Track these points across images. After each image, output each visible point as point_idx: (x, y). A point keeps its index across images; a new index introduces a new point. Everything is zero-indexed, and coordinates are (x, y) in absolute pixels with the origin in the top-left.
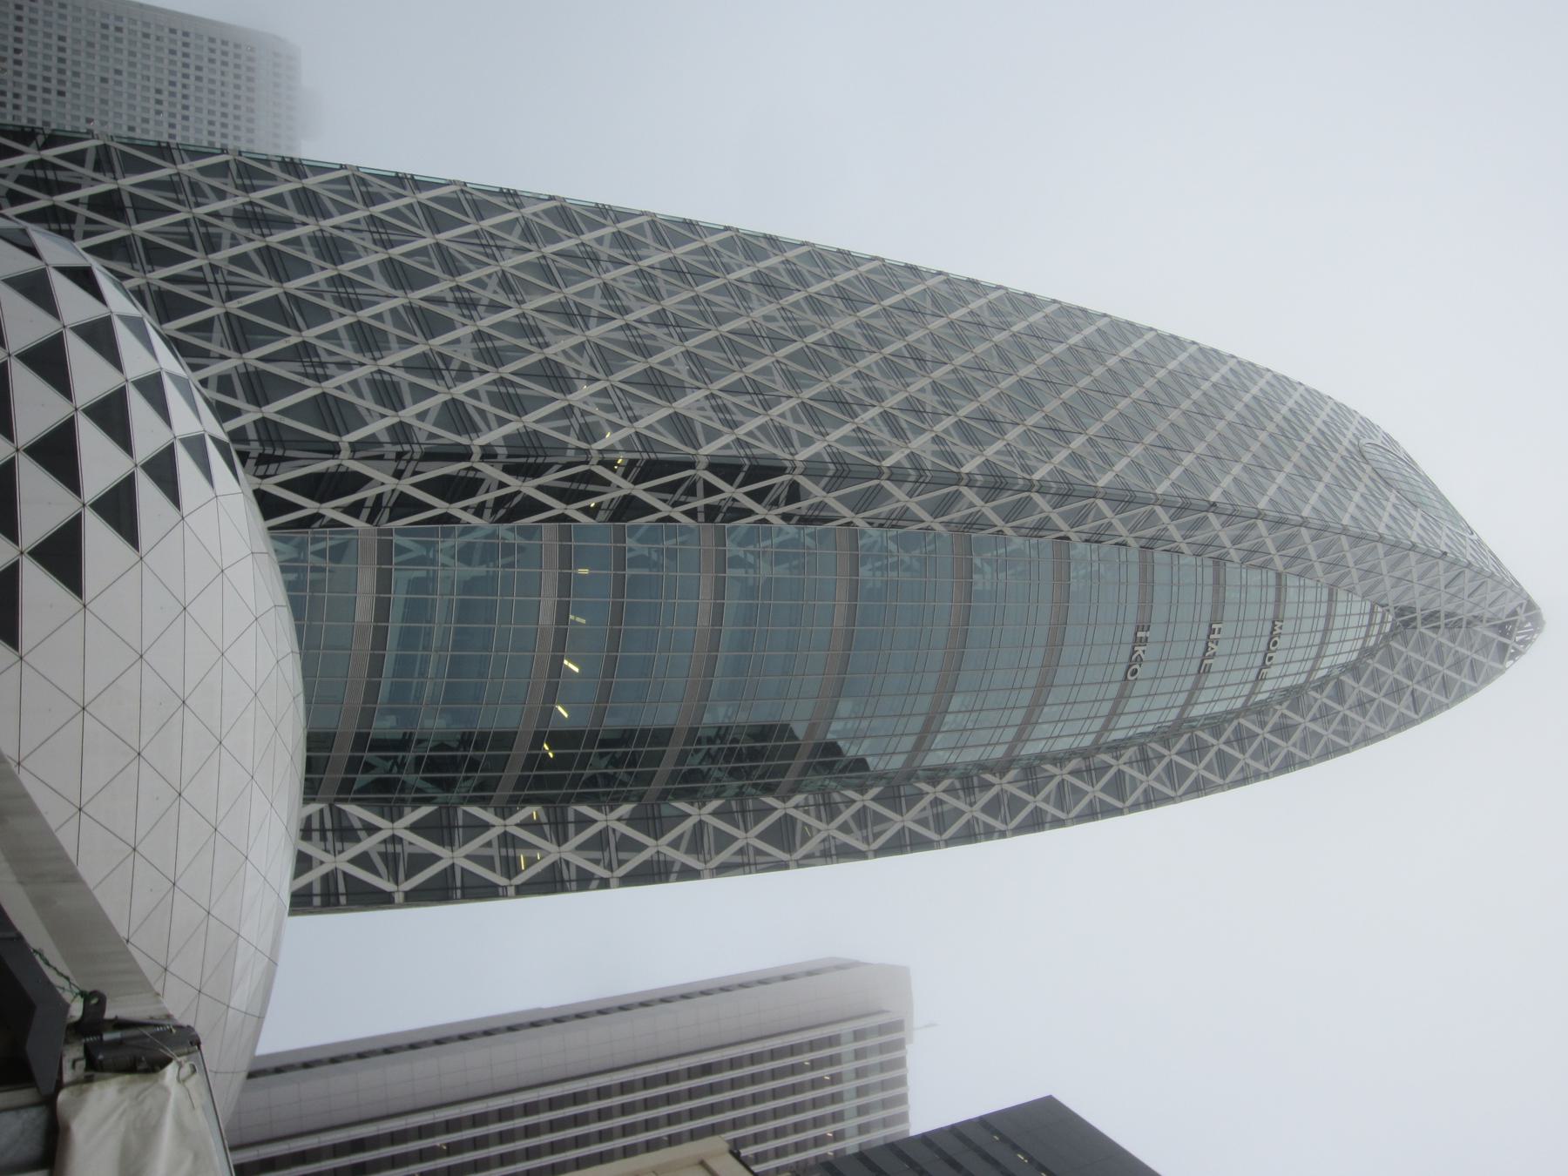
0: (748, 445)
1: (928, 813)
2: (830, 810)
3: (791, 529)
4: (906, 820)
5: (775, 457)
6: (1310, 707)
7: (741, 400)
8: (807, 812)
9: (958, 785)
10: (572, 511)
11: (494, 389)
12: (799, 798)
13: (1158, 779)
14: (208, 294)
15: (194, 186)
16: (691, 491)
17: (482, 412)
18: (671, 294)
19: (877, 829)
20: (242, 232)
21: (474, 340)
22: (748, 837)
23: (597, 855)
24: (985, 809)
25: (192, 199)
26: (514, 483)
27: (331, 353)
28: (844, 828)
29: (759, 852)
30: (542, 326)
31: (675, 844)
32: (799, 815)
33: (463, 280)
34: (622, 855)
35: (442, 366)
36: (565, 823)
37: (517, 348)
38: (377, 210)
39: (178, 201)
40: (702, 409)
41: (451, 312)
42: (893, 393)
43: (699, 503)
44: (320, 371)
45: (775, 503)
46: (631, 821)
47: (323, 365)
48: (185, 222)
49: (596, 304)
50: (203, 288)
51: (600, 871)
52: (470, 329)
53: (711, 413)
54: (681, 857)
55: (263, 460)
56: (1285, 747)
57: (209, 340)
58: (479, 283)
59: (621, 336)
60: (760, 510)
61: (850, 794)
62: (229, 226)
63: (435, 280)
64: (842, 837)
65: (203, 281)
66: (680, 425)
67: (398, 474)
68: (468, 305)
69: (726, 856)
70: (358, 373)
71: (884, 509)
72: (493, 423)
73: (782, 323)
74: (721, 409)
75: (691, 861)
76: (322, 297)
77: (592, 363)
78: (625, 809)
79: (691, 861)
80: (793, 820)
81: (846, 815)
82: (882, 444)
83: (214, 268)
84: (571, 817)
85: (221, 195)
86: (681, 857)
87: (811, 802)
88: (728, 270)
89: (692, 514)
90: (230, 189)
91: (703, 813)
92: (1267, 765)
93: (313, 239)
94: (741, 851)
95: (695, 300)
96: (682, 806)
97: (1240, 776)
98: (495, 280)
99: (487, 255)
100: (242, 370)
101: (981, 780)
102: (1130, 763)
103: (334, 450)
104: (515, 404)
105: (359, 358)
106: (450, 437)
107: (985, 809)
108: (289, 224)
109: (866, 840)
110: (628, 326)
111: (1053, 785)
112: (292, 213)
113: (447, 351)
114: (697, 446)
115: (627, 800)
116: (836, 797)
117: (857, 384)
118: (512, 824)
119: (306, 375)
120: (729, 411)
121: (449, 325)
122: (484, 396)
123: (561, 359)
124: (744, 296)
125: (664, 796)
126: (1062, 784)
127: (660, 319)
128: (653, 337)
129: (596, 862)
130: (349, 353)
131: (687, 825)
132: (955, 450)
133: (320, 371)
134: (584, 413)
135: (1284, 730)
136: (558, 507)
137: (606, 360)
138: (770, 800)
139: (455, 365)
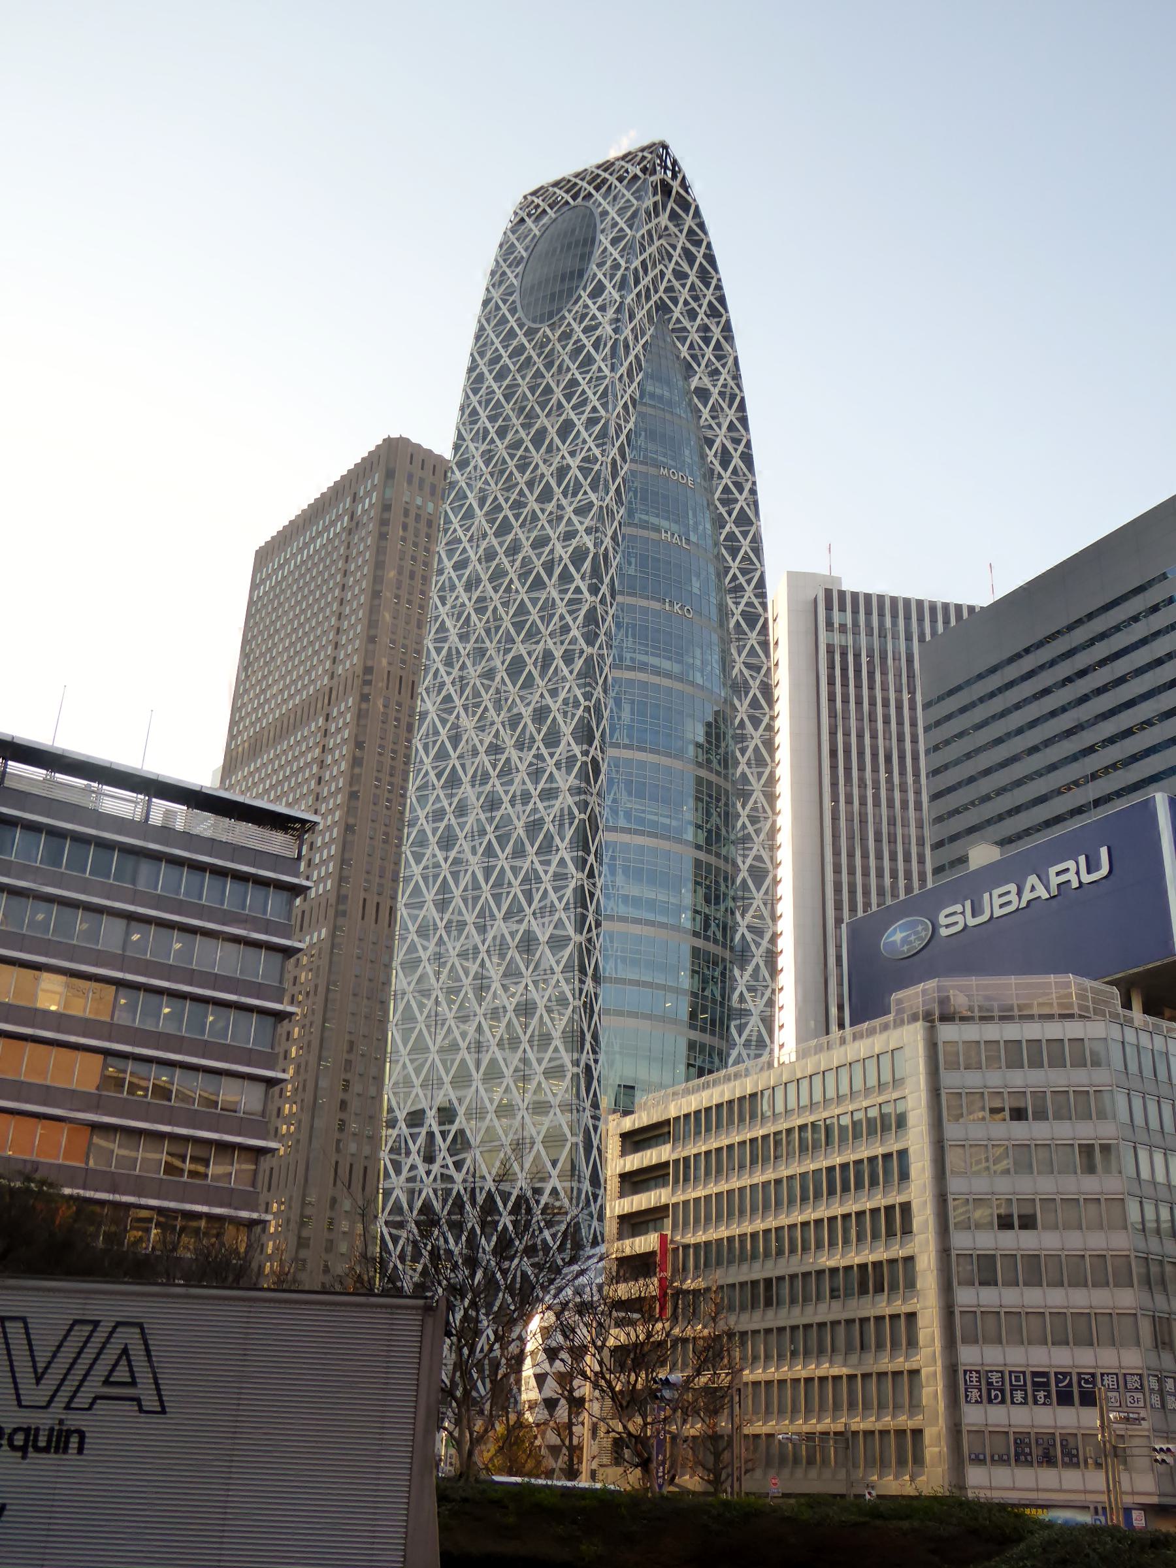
0: (567, 903)
1: (755, 770)
2: (747, 838)
3: (605, 869)
4: (757, 786)
5: (575, 890)
6: (710, 427)
7: (537, 897)
9: (740, 746)
10: (596, 1009)
11: (535, 1048)
12: (739, 860)
13: (749, 582)
14: (481, 1189)
15: (408, 1180)
16: (589, 940)
17: (551, 1060)
18: (460, 913)
19: (761, 810)
20: (439, 1162)
22: (758, 897)
23: (759, 993)
24: (756, 729)
25: (418, 1183)
26: (588, 1046)
29: (766, 893)
31: (758, 945)
32: (749, 861)
33: (463, 1045)
34: (761, 979)
36: (741, 1010)
38: (417, 1082)
39: (420, 1192)
40: (543, 924)
42: (524, 783)
45: (594, 885)
46: (742, 969)
48: (435, 1191)
49: (474, 968)
50: (478, 1190)
51: (768, 993)
52: (496, 1049)
53: (546, 920)
54: (765, 943)
55: (579, 1182)
56: (736, 461)
57: (510, 1194)
58: (464, 1035)
60: (598, 893)
61: (739, 824)
62: (436, 1168)
63: (463, 1061)
64: (762, 836)
65: (473, 1190)
66: (557, 943)
67: (584, 1109)
68: (479, 1047)
69: (766, 914)
70: (528, 1120)
72: (555, 1055)
73: (477, 843)
75: (768, 936)
77: (516, 983)
78: (737, 972)
79: (768, 936)
80: (751, 866)
81: (750, 829)
82: (562, 810)
83: (465, 1181)
84: (738, 1006)
85: (413, 1167)
86: (765, 943)
87: (741, 852)
88: (437, 865)
90: (410, 1161)
91: (743, 923)
92: (747, 480)
93: (441, 1123)
94: (765, 904)
95: (465, 900)
96: (738, 937)
97: (752, 507)
98: (462, 1026)
99: (443, 1025)
101: (738, 728)
102: (737, 604)
104: (544, 1040)
105: (519, 1117)
107: (756, 729)
108: (431, 1135)
109: (766, 818)
110: (488, 951)
111: (746, 672)
112: (423, 1131)
113: (512, 1069)
115: (731, 971)
116: (740, 835)
117: (519, 807)
118: (740, 1041)
121: (493, 1062)
122: (541, 1055)
123: (514, 1001)
124: (456, 862)
125: (732, 949)
126: (748, 666)
127: (482, 929)
128: (494, 938)
129: (763, 994)
131: (749, 936)
132: (564, 755)
134: (549, 1000)
135: (725, 458)
136: (596, 1017)
137: (511, 973)
138: (739, 880)
139: (521, 1066)
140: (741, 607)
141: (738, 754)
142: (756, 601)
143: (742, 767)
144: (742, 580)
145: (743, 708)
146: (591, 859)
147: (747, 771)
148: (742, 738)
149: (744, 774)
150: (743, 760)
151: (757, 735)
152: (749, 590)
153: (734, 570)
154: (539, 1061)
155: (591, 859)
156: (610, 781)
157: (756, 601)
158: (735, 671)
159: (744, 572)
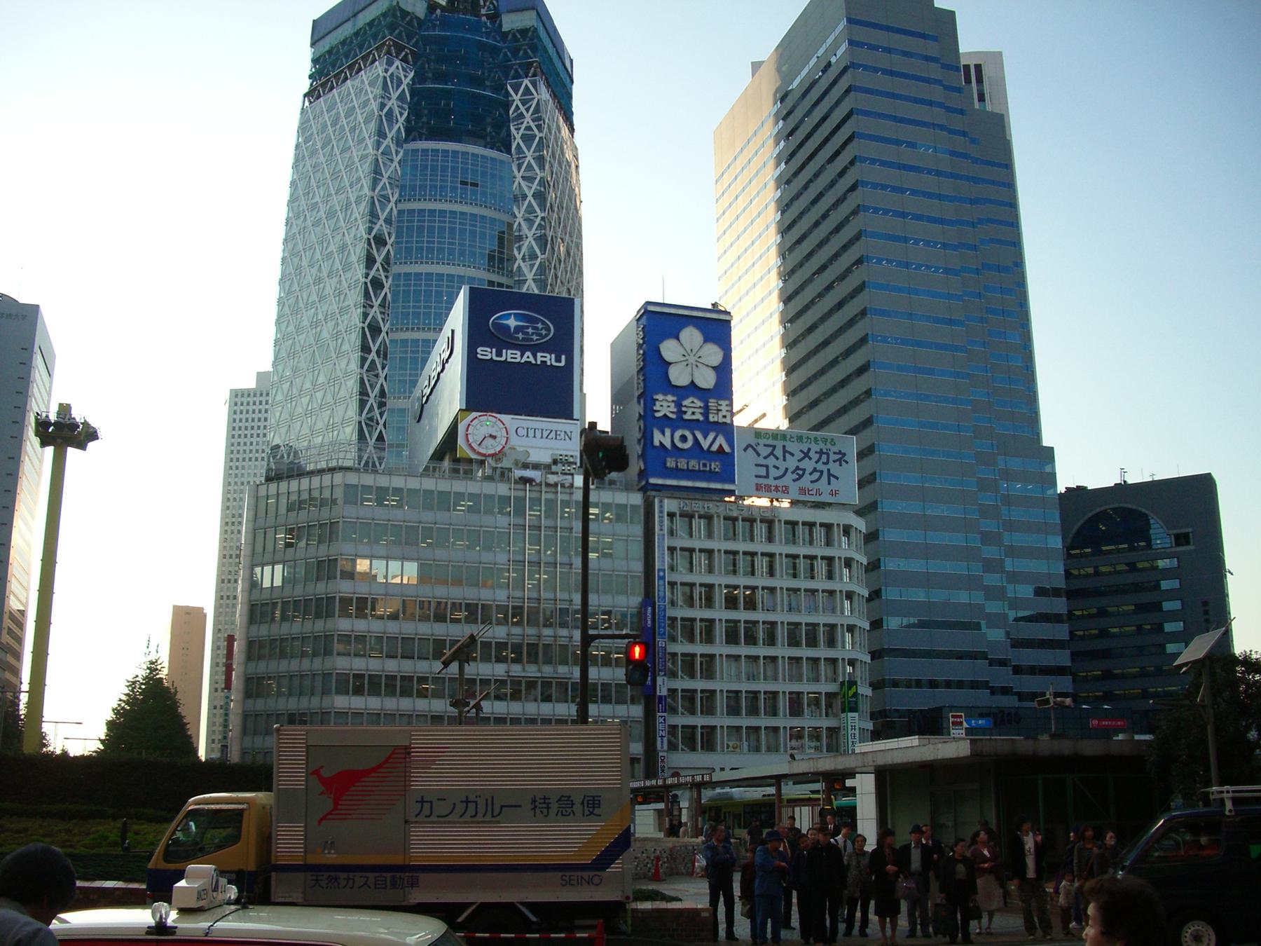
13: (527, 110)
16: (371, 419)
24: (530, 229)
43: (377, 412)
71: (379, 317)
89: (381, 414)
140: (521, 131)
141: (516, 252)
142: (533, 125)
143: (519, 261)
144: (522, 109)
145: (520, 213)
146: (373, 355)
147: (522, 265)
148: (520, 238)
149: (519, 267)
150: (519, 257)
151: (530, 234)
152: (528, 116)
153: (517, 102)
155: (373, 355)
156: (395, 294)
157: (533, 125)
158: (516, 184)
159: (524, 102)
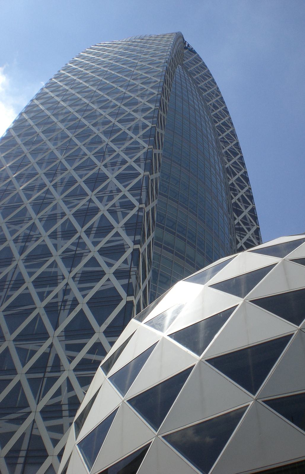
8: (243, 238)
17: (108, 242)
21: (56, 238)
27: (56, 296)
28: (249, 229)
30: (49, 213)
35: (74, 253)
37: (63, 225)
41: (32, 247)
44: (69, 303)
47: (64, 302)
53: (116, 168)
59: (60, 189)
74: (113, 164)
76: (10, 296)
87: (239, 235)
100: (63, 338)
101: (231, 185)
103: (130, 304)
106: (127, 254)
114: (139, 174)
119: (71, 310)
120: (116, 162)
128: (63, 179)
130: (58, 289)
133: (69, 303)
154: (95, 244)
